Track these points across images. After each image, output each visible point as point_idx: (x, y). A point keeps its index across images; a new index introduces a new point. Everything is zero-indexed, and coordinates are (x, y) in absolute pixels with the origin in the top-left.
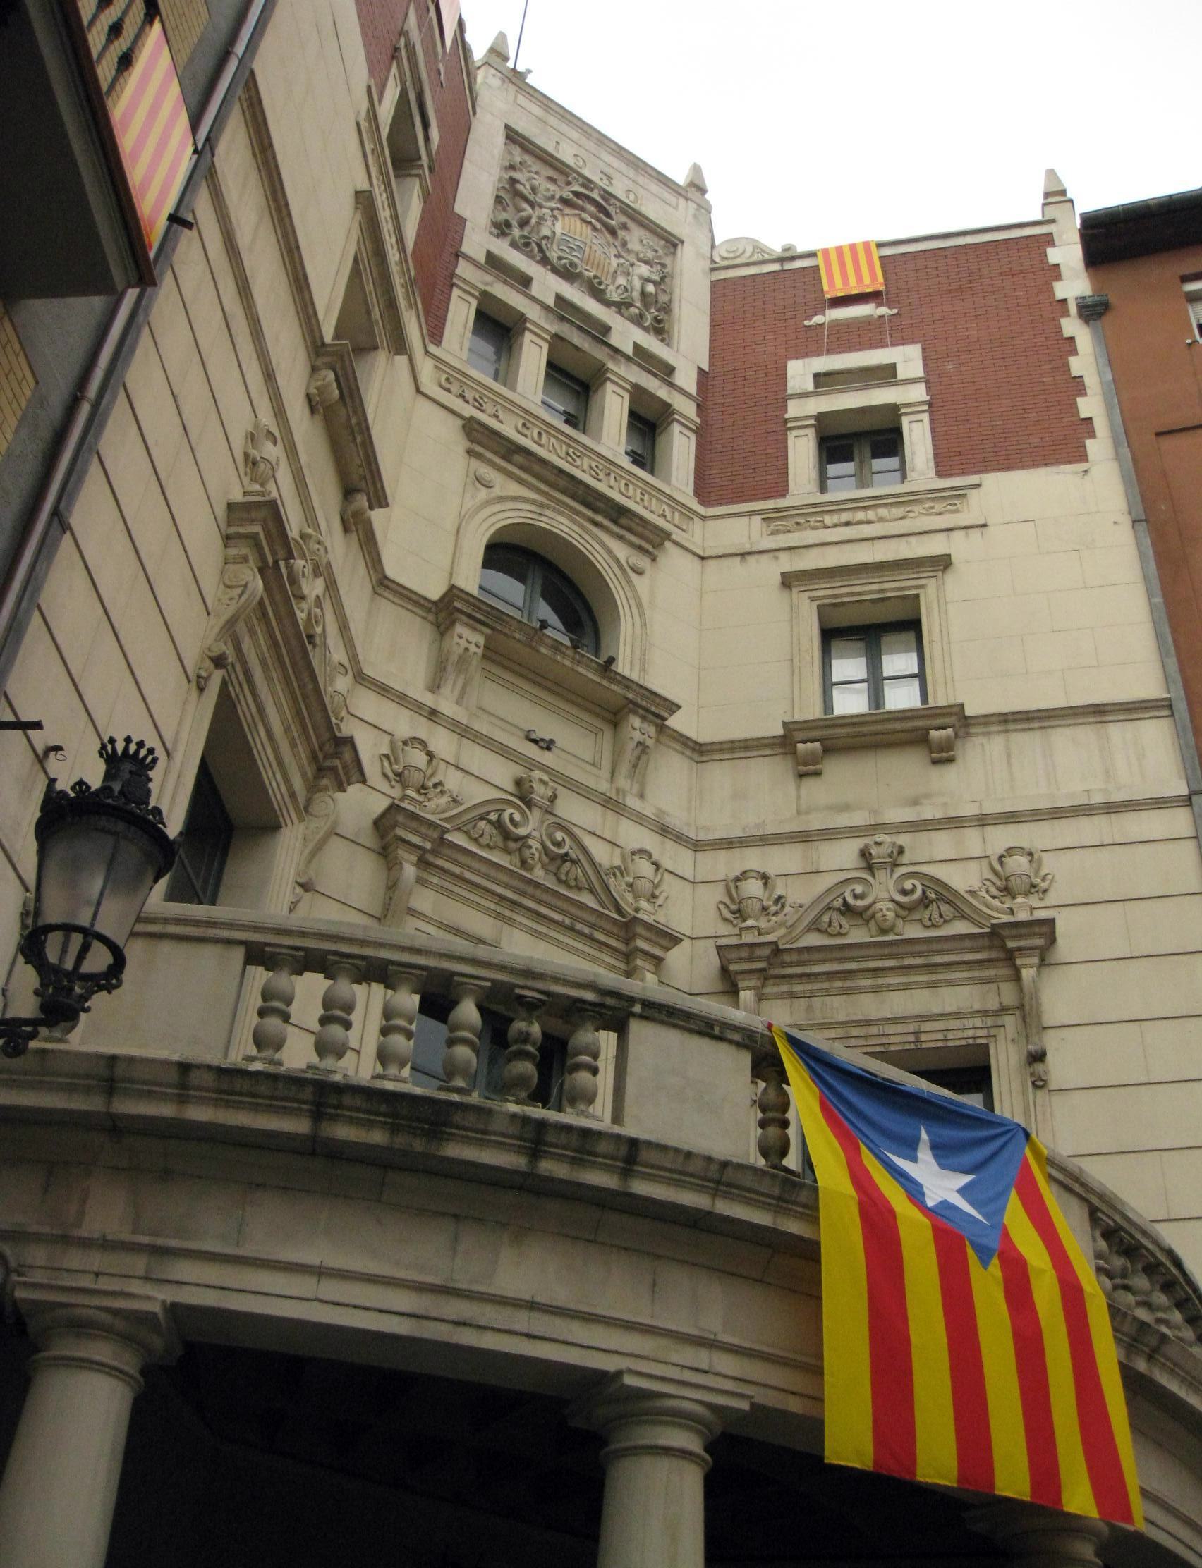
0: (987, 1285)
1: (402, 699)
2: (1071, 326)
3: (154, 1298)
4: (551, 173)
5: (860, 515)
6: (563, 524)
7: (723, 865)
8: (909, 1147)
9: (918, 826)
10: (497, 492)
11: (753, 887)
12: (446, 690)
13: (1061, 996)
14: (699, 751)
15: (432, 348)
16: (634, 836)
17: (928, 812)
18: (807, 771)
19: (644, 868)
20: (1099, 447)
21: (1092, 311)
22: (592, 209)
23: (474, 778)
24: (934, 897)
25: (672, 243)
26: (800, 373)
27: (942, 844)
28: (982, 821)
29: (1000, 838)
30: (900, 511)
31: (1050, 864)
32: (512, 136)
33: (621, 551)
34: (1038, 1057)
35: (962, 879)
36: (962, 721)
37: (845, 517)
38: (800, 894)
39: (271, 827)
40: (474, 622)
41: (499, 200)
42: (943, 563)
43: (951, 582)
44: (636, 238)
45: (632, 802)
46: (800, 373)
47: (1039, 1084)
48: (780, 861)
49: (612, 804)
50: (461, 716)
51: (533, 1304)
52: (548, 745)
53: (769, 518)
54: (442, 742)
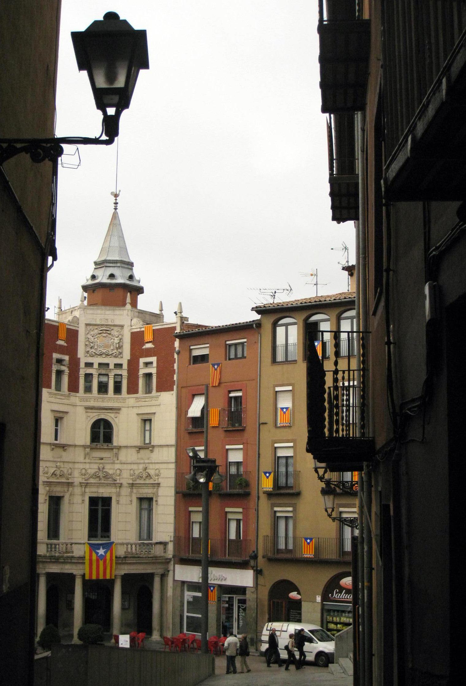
0: (101, 563)
1: (81, 463)
2: (176, 356)
3: (44, 572)
4: (96, 327)
5: (147, 400)
6: (102, 417)
7: (130, 467)
8: (99, 549)
9: (149, 463)
10: (91, 417)
11: (132, 472)
12: (87, 458)
13: (161, 491)
14: (126, 447)
15: (77, 394)
16: (117, 466)
17: (150, 462)
18: (138, 452)
19: (118, 472)
20: (175, 387)
21: (178, 353)
22: (104, 332)
23: (92, 468)
24: (149, 476)
25: (122, 326)
26: (142, 360)
27: (151, 466)
28: (155, 463)
29: (157, 466)
30: (151, 399)
31: (162, 471)
32: (87, 325)
33: (112, 415)
34: (156, 501)
35: (152, 472)
36: (153, 446)
37: (144, 400)
38: (137, 473)
39: (63, 497)
40: (88, 448)
41: (86, 345)
42: (155, 413)
43: (156, 415)
44: (115, 333)
45: (116, 462)
46: (142, 360)
47: (157, 504)
48: (135, 467)
49: (113, 463)
50: (89, 461)
51: (68, 569)
52: (102, 459)
53: (137, 398)
54: (87, 466)
